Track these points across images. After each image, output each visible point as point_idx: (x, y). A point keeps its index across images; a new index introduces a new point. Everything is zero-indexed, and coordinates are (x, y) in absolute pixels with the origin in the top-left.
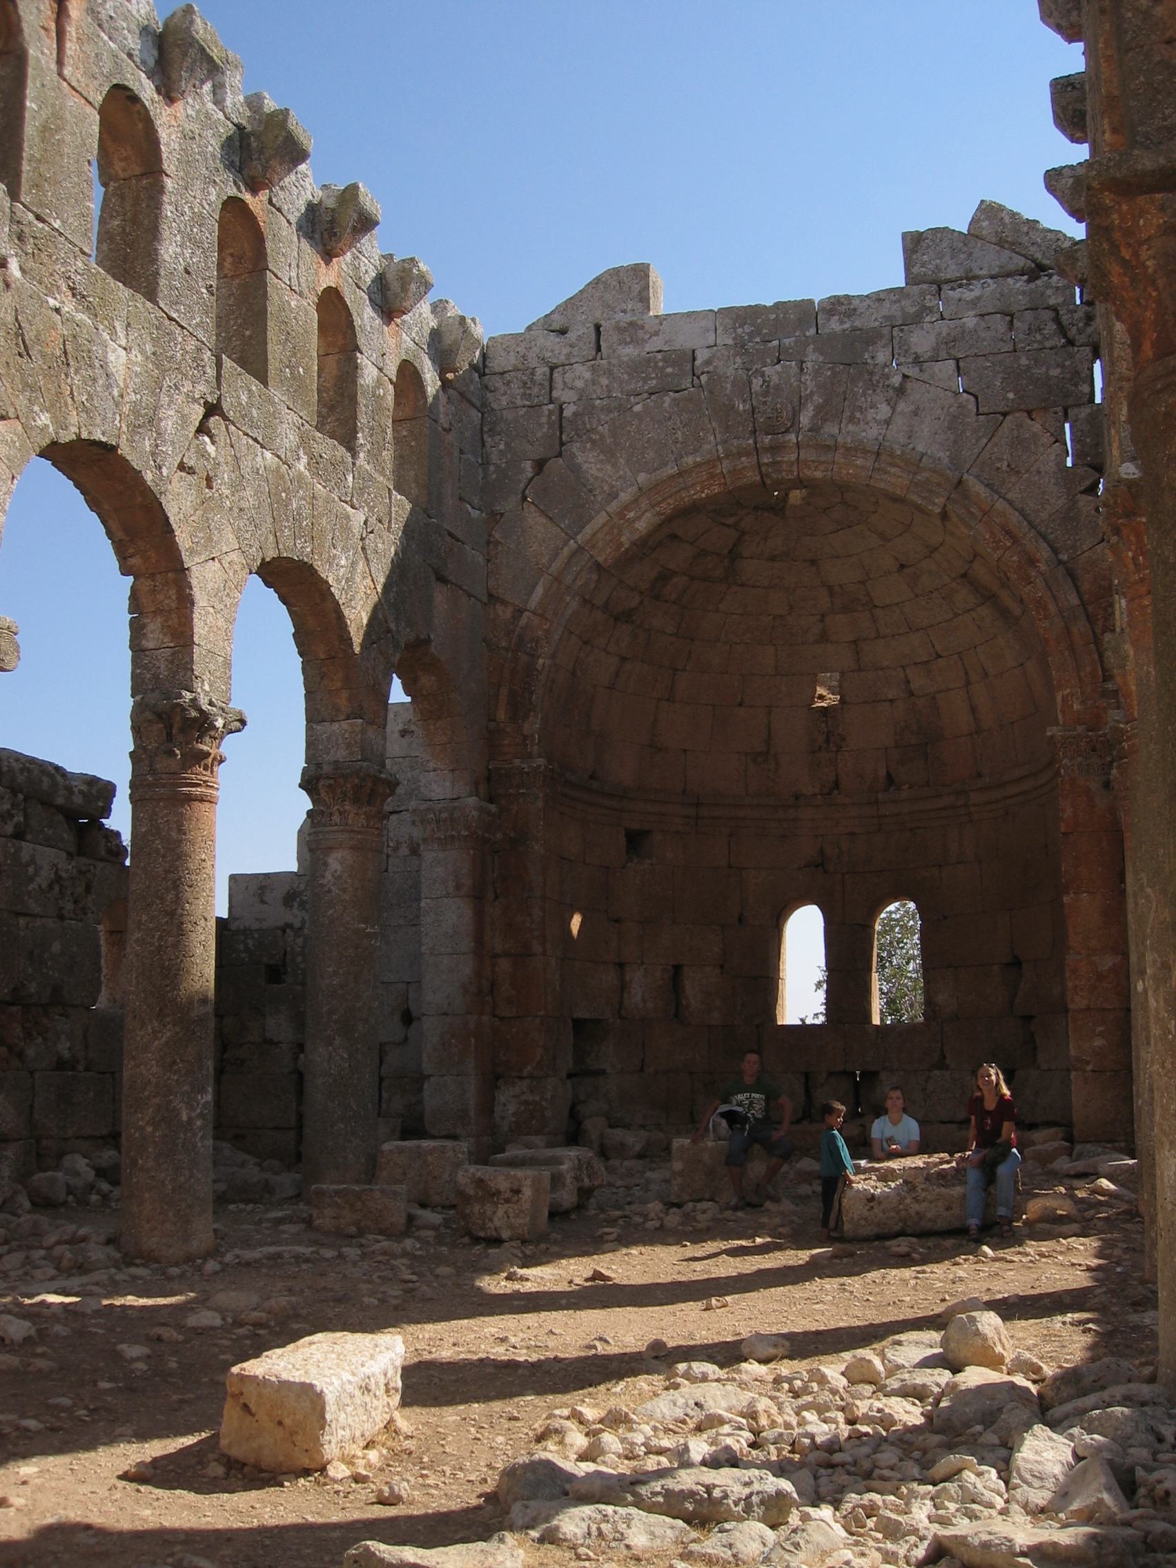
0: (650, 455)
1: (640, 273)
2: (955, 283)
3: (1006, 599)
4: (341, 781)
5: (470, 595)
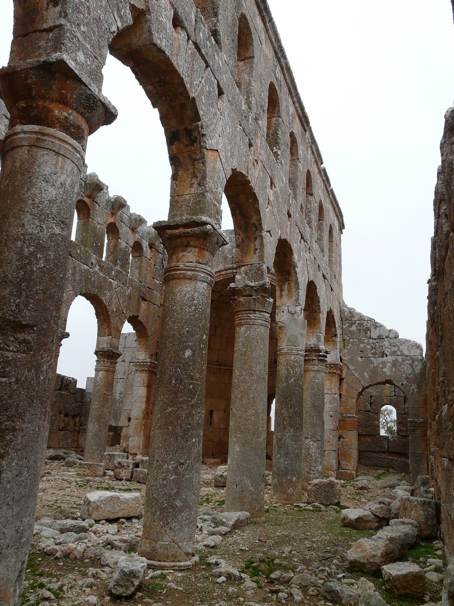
5: (154, 304)
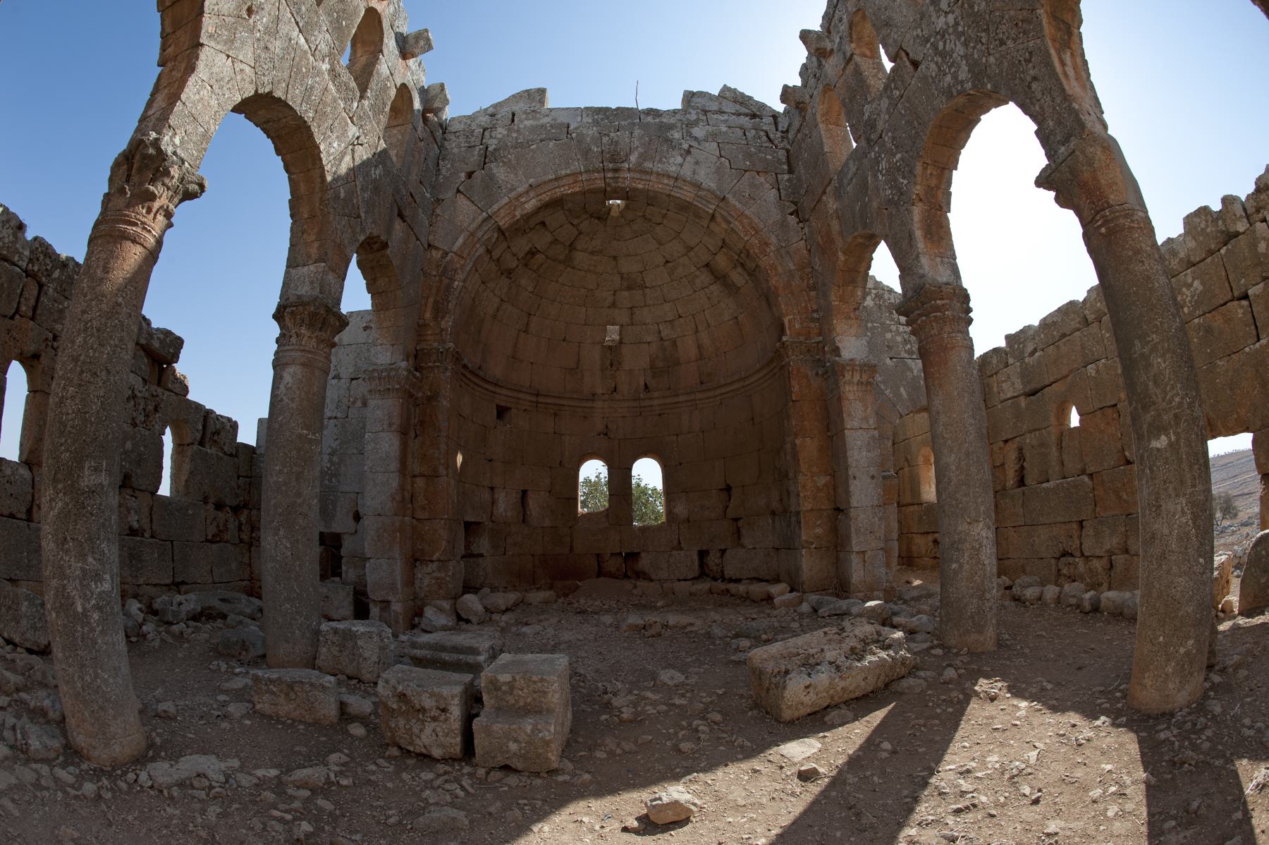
0: (538, 170)
1: (542, 92)
2: (716, 112)
3: (737, 277)
4: (301, 308)
